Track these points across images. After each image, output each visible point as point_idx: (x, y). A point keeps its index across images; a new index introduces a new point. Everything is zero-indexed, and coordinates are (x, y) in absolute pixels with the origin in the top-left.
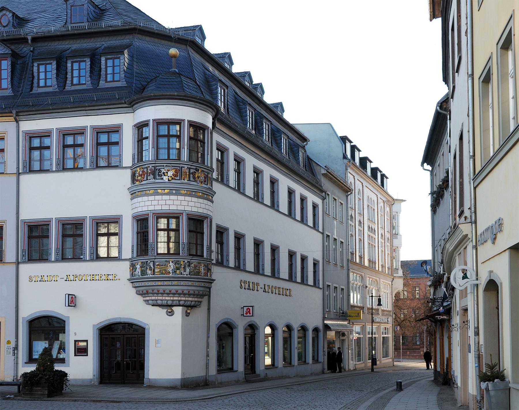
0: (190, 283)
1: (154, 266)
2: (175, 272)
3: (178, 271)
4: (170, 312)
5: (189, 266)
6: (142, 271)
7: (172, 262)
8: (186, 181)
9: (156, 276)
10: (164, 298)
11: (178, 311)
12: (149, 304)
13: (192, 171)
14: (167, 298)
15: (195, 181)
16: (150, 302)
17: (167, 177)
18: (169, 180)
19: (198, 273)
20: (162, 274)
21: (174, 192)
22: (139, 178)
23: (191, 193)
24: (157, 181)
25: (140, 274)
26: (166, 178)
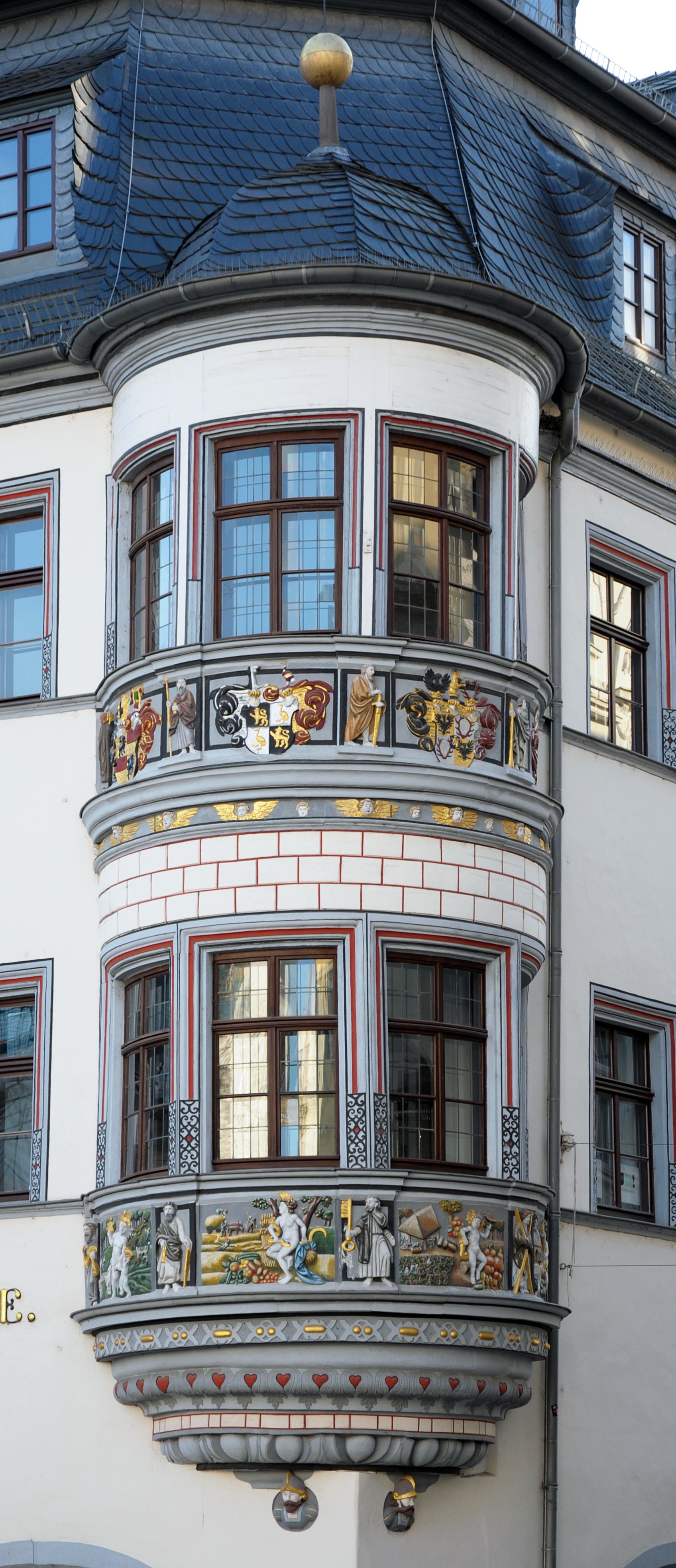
0: (395, 1330)
2: (306, 1264)
4: (292, 1507)
5: (389, 1226)
7: (293, 1208)
8: (369, 747)
9: (204, 1290)
10: (253, 1421)
11: (339, 1493)
12: (184, 1461)
13: (404, 689)
14: (271, 1422)
15: (426, 745)
16: (186, 1445)
17: (265, 732)
18: (273, 749)
19: (447, 1269)
20: (237, 1276)
21: (302, 810)
23: (404, 813)
24: (212, 757)
25: (124, 1279)
26: (256, 739)
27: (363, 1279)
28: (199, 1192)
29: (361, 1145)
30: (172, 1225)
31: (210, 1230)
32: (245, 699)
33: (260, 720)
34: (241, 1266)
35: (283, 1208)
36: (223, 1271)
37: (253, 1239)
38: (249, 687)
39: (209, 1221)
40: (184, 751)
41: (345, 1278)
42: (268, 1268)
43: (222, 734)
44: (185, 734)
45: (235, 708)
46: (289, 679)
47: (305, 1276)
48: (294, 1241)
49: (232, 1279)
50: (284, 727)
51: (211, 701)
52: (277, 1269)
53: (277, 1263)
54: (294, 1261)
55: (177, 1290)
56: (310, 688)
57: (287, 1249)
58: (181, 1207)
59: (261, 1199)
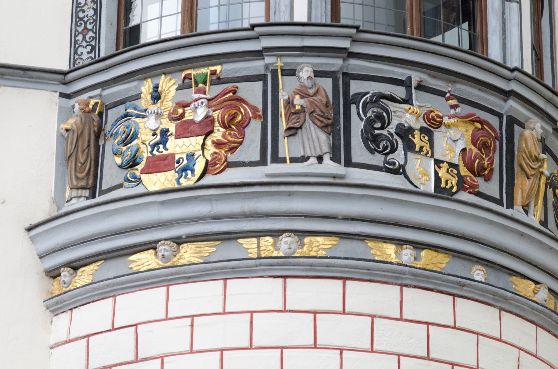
22: (177, 147)
32: (405, 116)
33: (421, 148)
38: (408, 101)
40: (313, 160)
43: (372, 151)
44: (316, 139)
45: (389, 124)
46: (453, 107)
50: (451, 165)
51: (353, 107)
56: (478, 125)
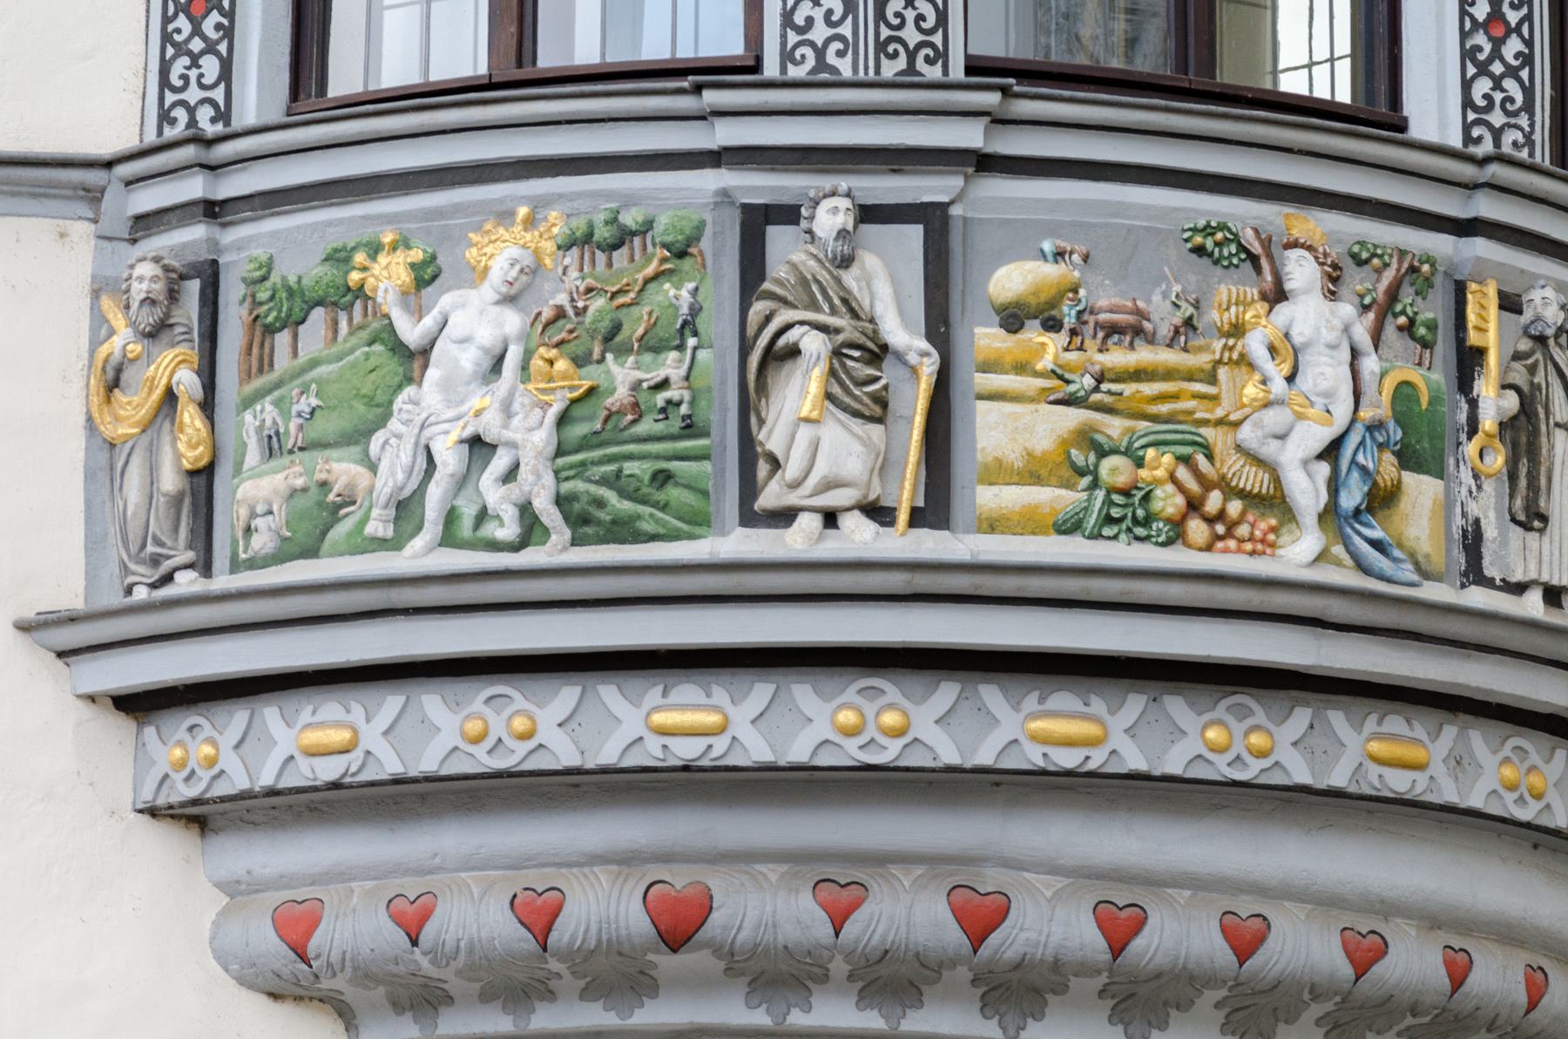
1: (939, 325)
3: (1421, 490)
6: (582, 431)
7: (1333, 280)
20: (1128, 513)
27: (1519, 589)
28: (986, 163)
29: (1510, 85)
30: (850, 278)
31: (1012, 318)
34: (1143, 473)
35: (1301, 271)
36: (1069, 486)
37: (1190, 377)
39: (1013, 279)
41: (1474, 574)
42: (1242, 494)
47: (1377, 545)
48: (1342, 410)
49: (1110, 520)
52: (1274, 502)
53: (1277, 480)
54: (1334, 486)
55: (860, 537)
57: (1316, 435)
58: (869, 214)
59: (1222, 227)
